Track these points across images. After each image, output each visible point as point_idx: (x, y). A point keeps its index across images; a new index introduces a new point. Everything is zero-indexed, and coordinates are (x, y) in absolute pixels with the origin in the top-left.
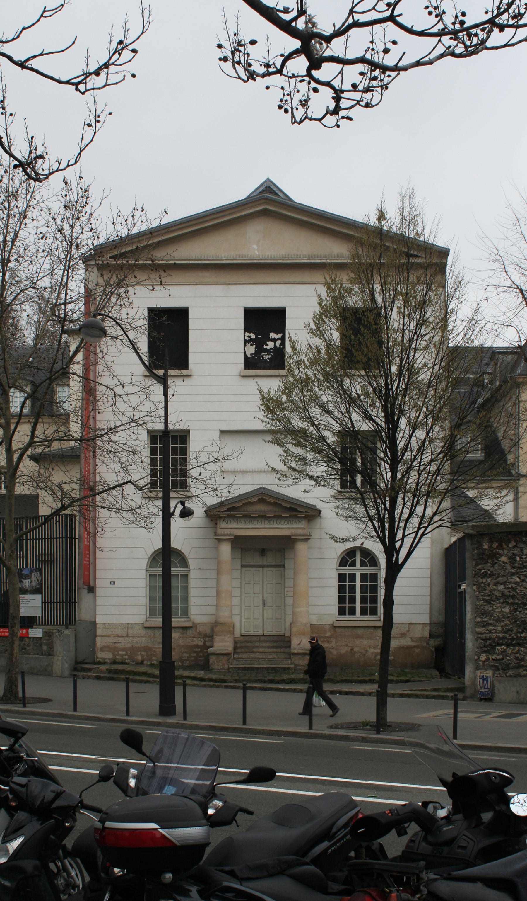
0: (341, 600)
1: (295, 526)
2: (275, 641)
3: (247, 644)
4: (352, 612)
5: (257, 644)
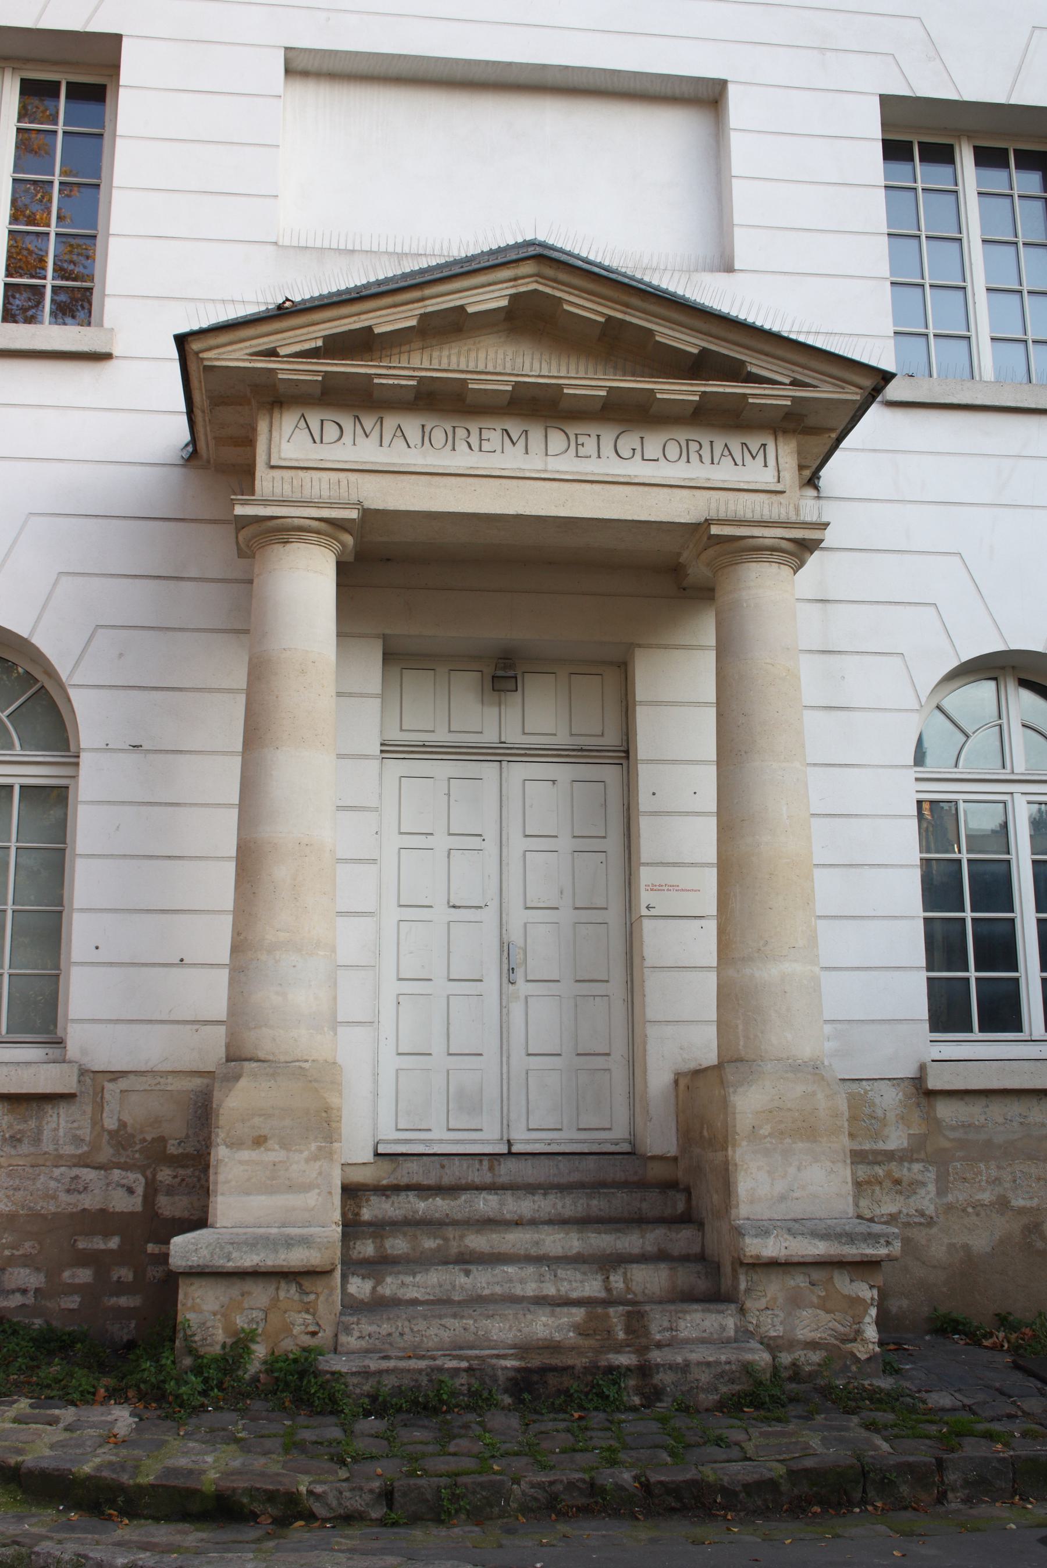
0: (943, 946)
1: (724, 473)
2: (596, 1186)
3: (422, 1206)
4: (1002, 1013)
5: (486, 1204)
